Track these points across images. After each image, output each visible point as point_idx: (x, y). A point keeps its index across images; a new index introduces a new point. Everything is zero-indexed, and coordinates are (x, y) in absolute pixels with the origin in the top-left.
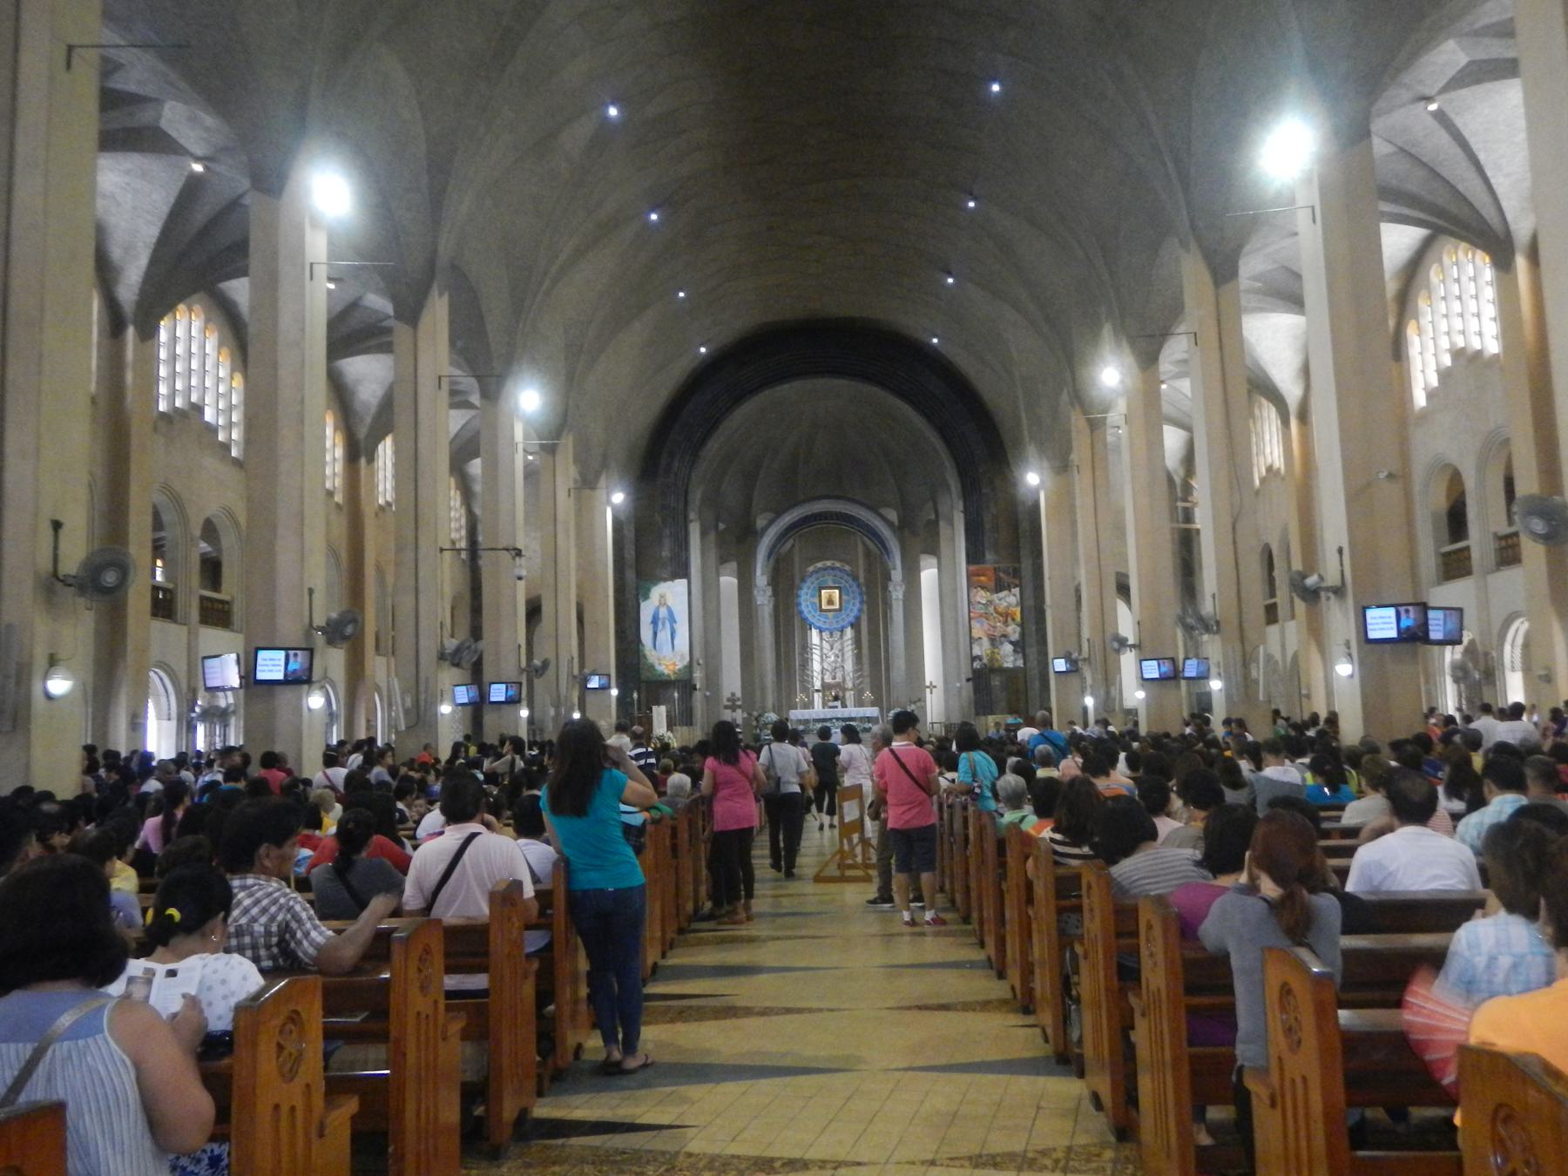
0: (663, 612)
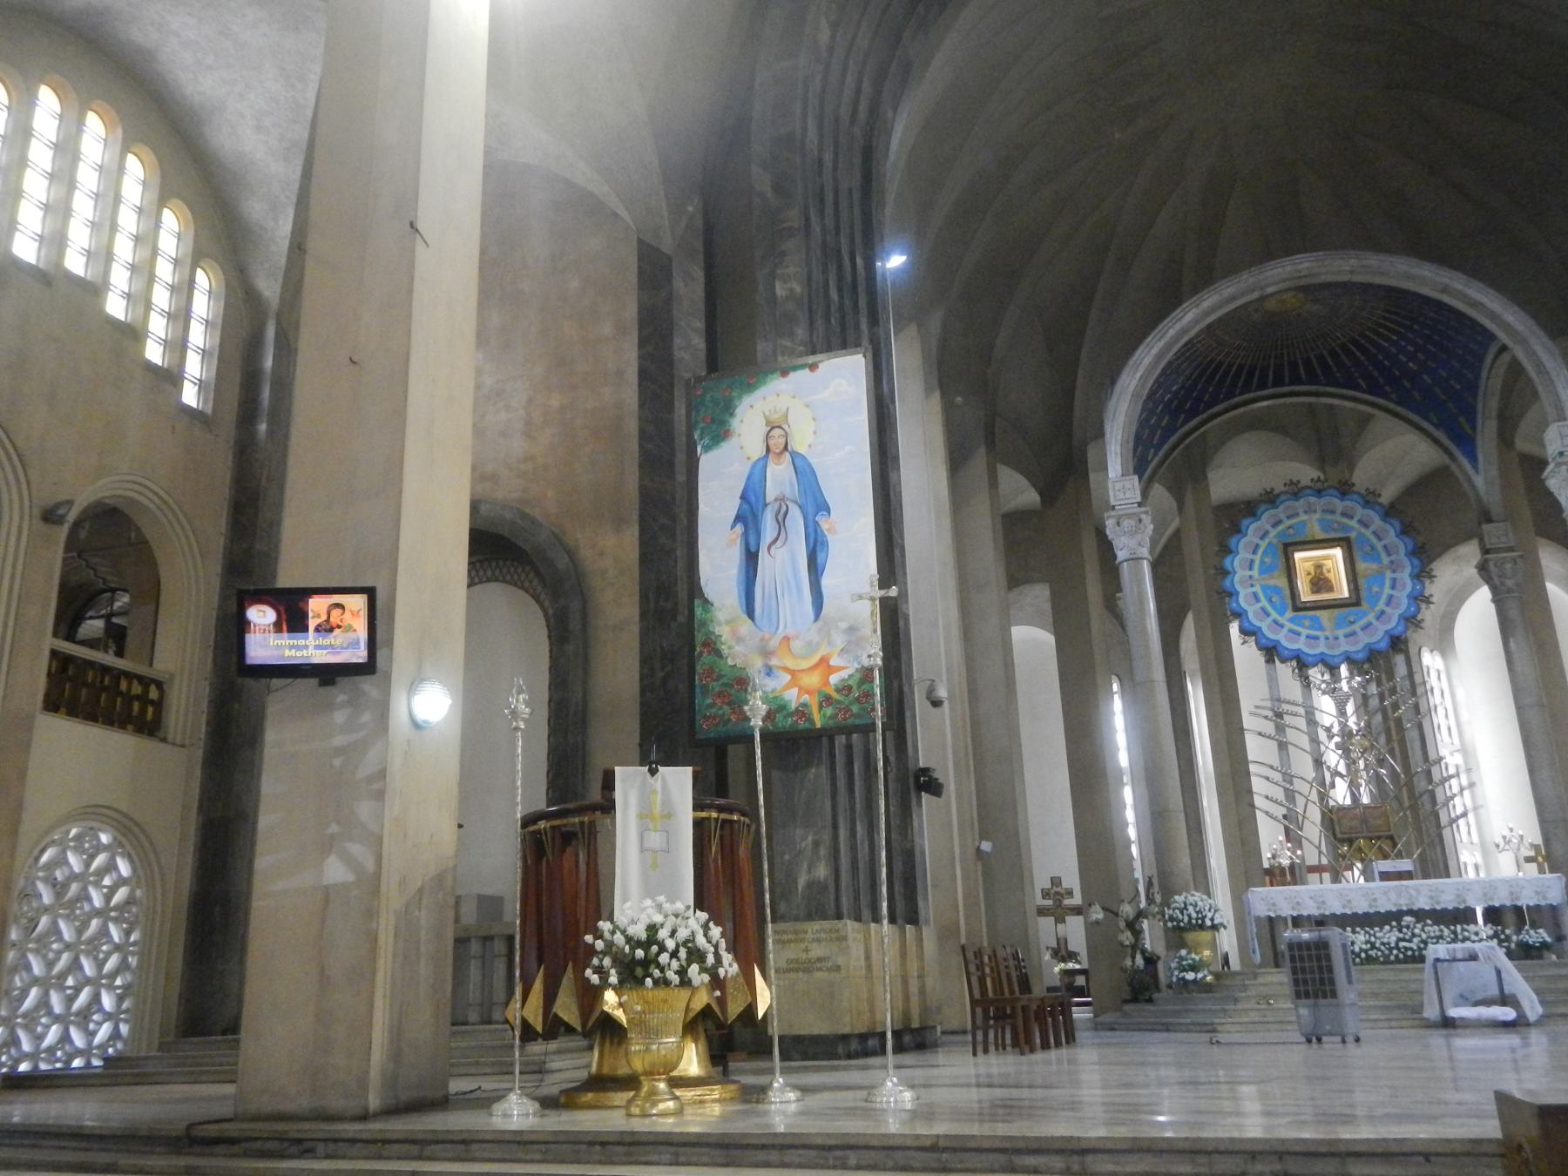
0: (779, 477)
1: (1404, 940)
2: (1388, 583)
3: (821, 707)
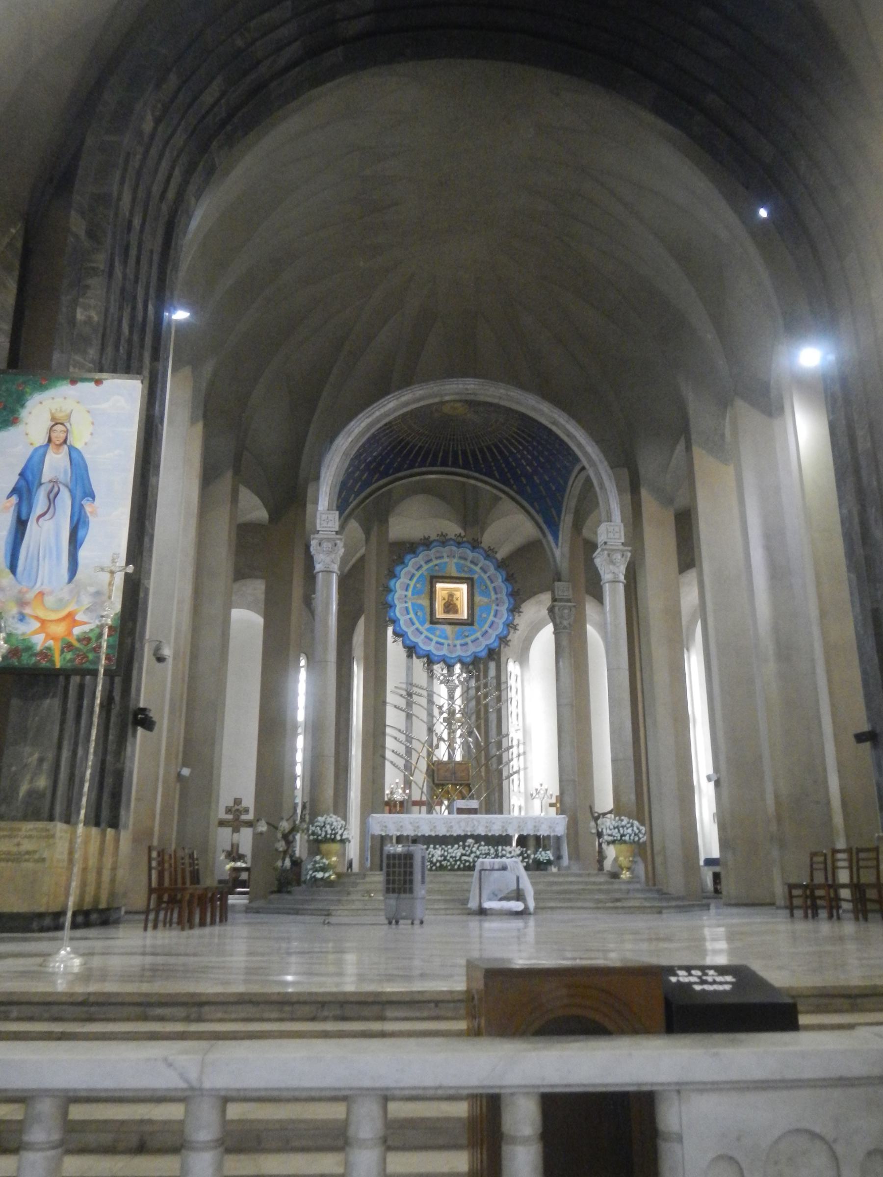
0: (55, 464)
1: (465, 855)
2: (492, 613)
3: (62, 652)
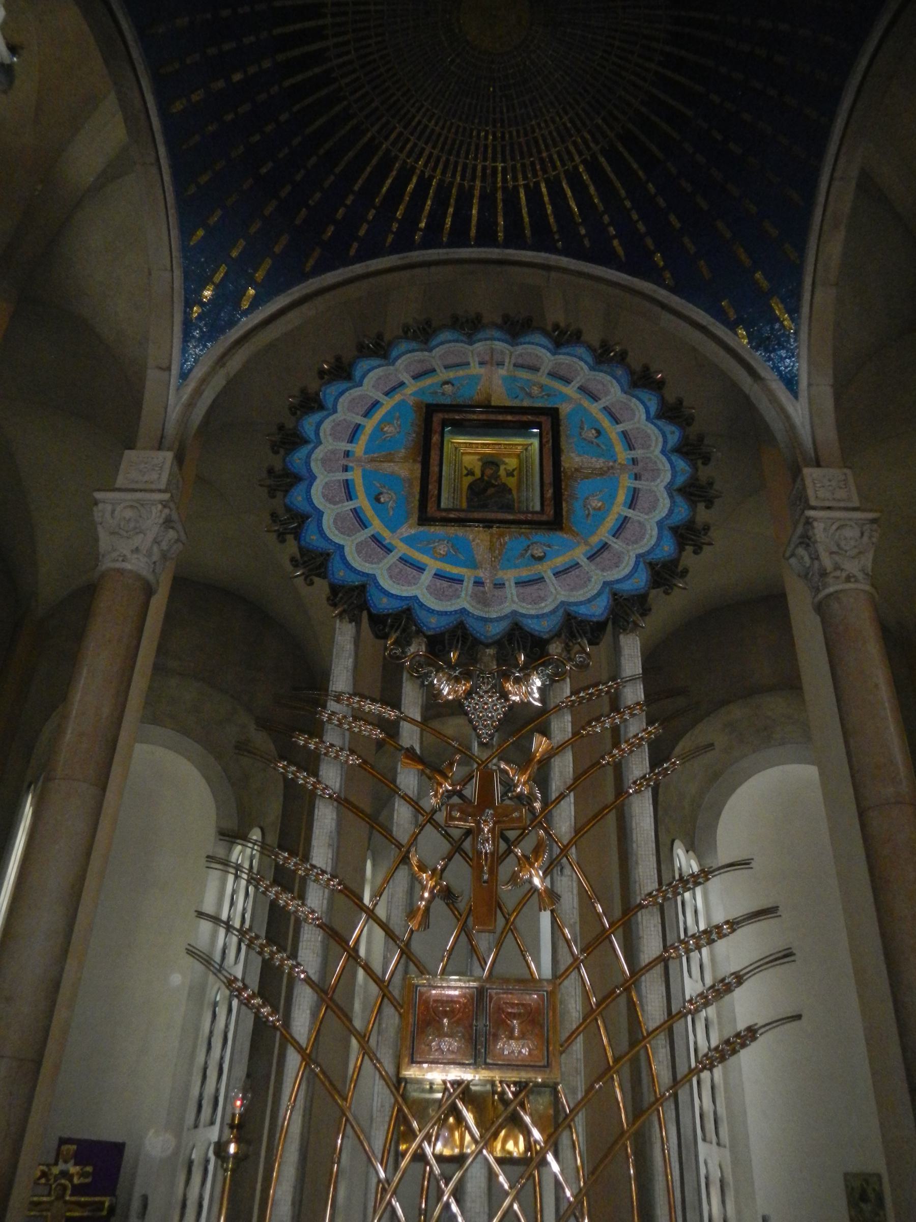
2: (621, 497)
